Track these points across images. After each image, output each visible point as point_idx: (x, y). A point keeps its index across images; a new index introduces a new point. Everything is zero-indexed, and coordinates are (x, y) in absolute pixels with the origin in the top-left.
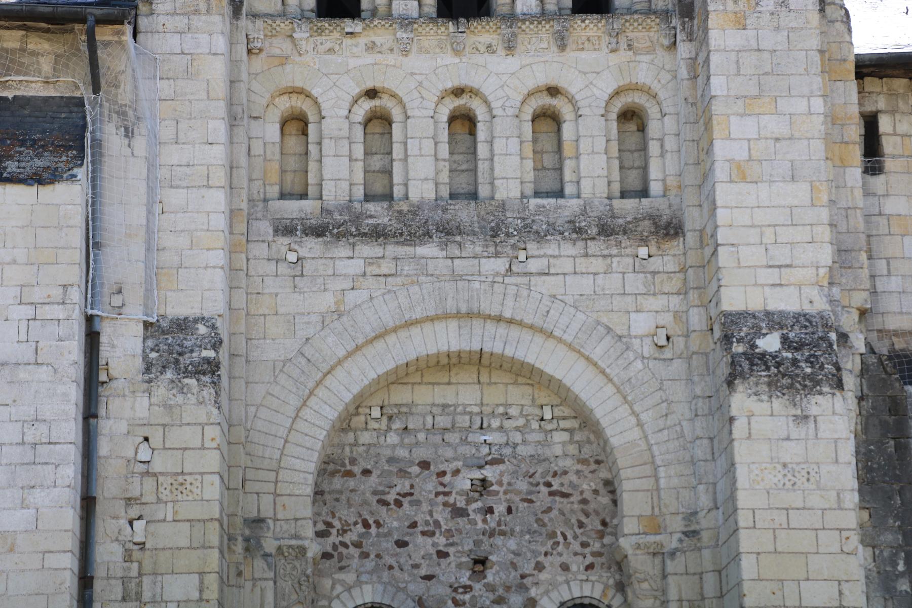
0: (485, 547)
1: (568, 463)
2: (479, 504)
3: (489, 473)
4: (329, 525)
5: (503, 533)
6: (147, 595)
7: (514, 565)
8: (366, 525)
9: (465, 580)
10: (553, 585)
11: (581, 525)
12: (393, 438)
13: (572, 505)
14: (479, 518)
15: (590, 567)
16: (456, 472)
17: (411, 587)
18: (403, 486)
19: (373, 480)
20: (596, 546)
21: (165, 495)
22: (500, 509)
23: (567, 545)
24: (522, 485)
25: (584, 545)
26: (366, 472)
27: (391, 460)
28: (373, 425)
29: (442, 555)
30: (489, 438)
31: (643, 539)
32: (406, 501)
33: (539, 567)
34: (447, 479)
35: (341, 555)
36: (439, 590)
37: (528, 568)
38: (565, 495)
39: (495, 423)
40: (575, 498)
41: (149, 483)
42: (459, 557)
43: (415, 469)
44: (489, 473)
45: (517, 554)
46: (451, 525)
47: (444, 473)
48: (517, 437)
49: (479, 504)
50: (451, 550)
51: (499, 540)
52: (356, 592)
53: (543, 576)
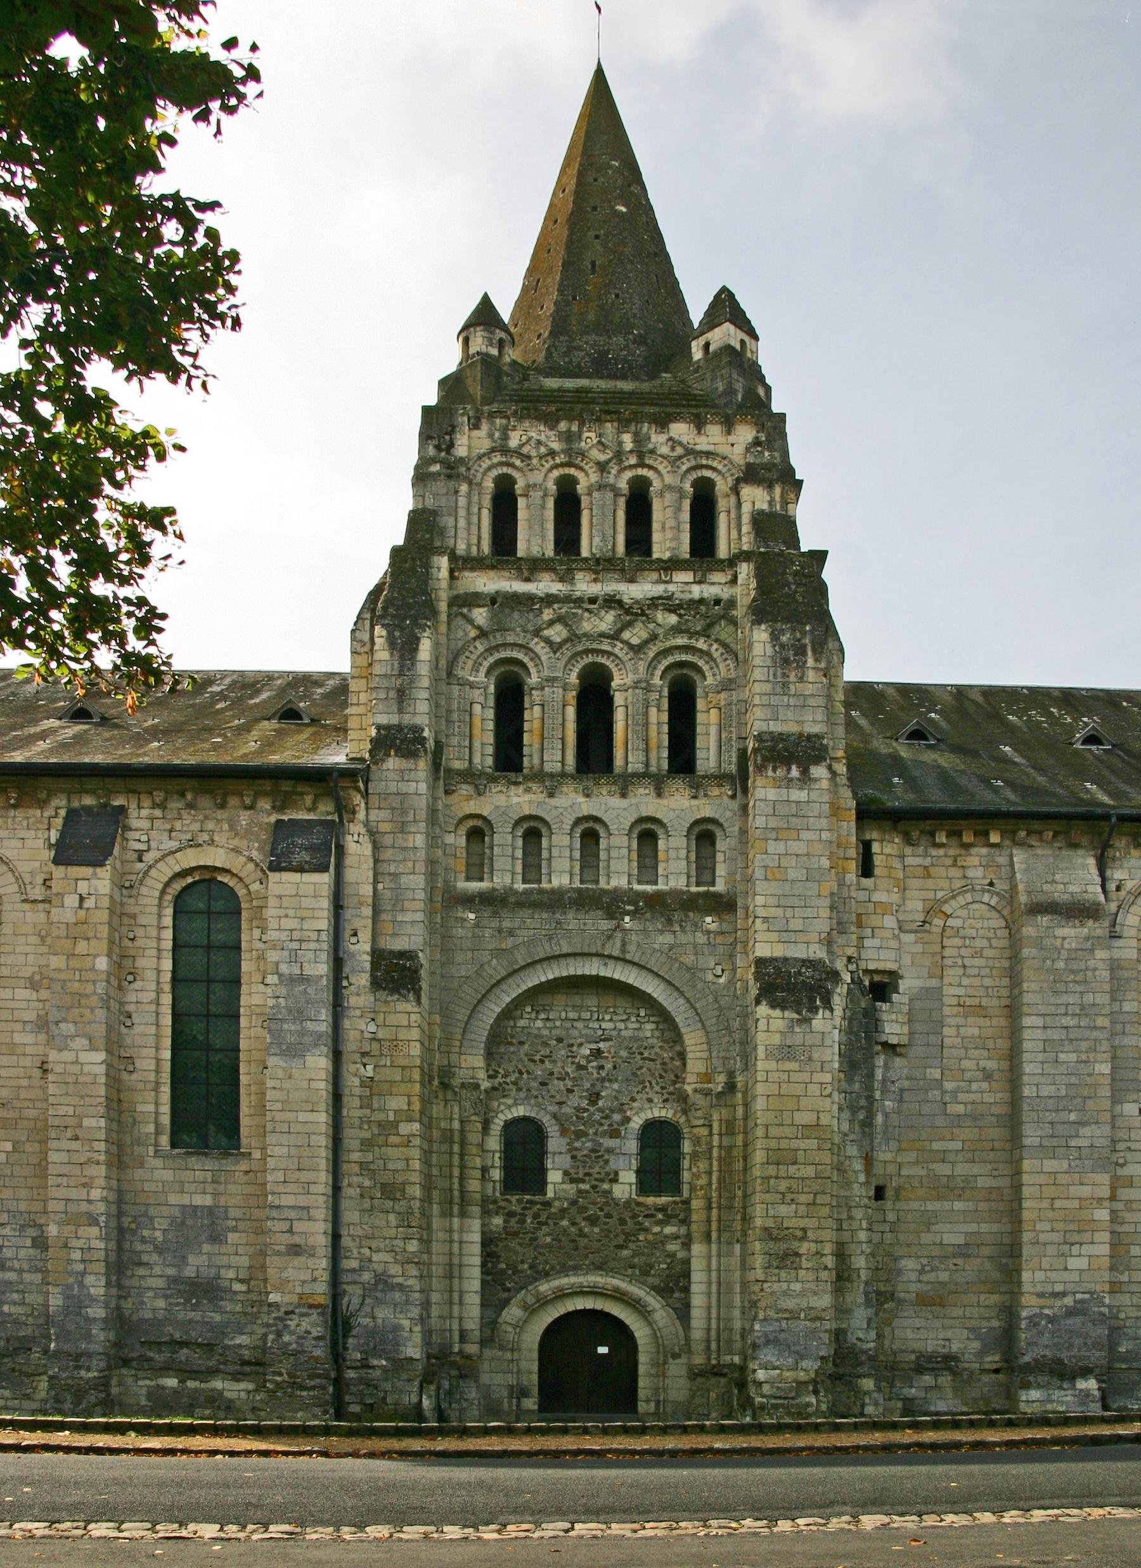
0: (598, 1087)
2: (594, 1064)
3: (601, 1045)
4: (497, 1072)
5: (610, 1081)
7: (616, 1098)
8: (521, 1073)
10: (642, 1109)
11: (661, 1077)
12: (539, 1024)
14: (595, 1072)
16: (581, 1045)
22: (609, 1066)
23: (652, 1087)
24: (624, 1053)
29: (570, 1091)
30: (604, 1025)
33: (633, 1100)
35: (504, 1090)
36: (566, 1110)
39: (607, 1017)
44: (601, 1045)
45: (618, 1092)
49: (594, 1064)
51: (607, 1084)
52: (513, 1109)
53: (635, 1105)
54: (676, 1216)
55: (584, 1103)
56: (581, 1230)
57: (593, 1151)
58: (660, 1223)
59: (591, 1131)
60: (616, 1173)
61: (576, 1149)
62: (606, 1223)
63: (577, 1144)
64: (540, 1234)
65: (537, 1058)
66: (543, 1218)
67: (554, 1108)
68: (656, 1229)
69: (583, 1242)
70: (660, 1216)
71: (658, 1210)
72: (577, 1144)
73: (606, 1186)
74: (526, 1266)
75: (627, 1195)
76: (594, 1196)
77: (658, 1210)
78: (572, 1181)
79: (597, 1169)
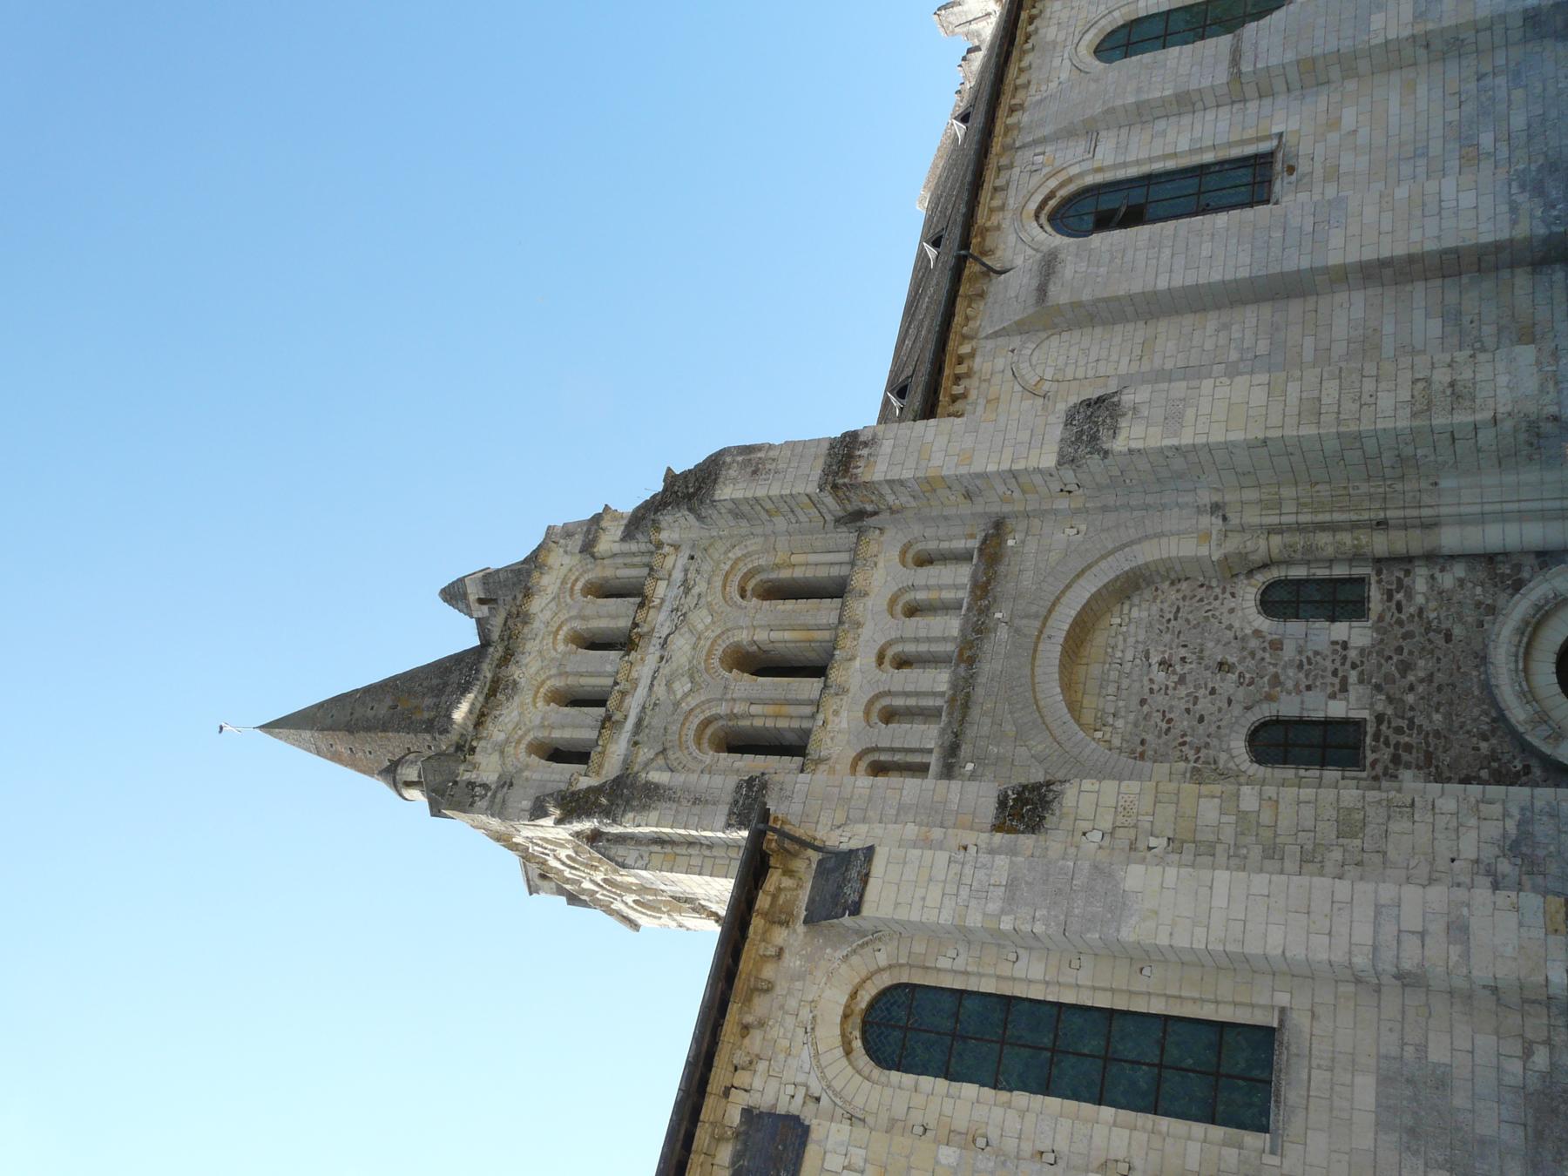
1: (1155, 609)
3: (1155, 660)
5: (1202, 651)
6: (1212, 838)
9: (1234, 677)
11: (1201, 600)
13: (1186, 607)
14: (1188, 667)
15: (1233, 595)
16: (1151, 681)
17: (1236, 713)
18: (1157, 717)
19: (1149, 737)
20: (1218, 591)
21: (1131, 821)
22: (1183, 652)
24: (1167, 637)
25: (1216, 598)
26: (1143, 742)
27: (1136, 725)
28: (1107, 737)
29: (1213, 692)
31: (1213, 543)
32: (1168, 716)
33: (1230, 627)
34: (1155, 687)
37: (1230, 634)
38: (1178, 609)
39: (1119, 654)
40: (1181, 603)
41: (1120, 833)
42: (1215, 681)
43: (1146, 708)
44: (1155, 660)
45: (1218, 641)
46: (1191, 685)
47: (1151, 691)
48: (1131, 640)
50: (1210, 685)
51: (1206, 653)
52: (1235, 753)
53: (1237, 625)
54: (1399, 579)
55: (1233, 677)
56: (1421, 681)
57: (1300, 666)
58: (1410, 596)
59: (1272, 669)
60: (1334, 643)
61: (1297, 685)
62: (1411, 653)
63: (1290, 684)
64: (1427, 726)
65: (1164, 726)
66: (1404, 724)
67: (1237, 710)
68: (1420, 600)
69: (1440, 677)
70: (1399, 596)
71: (1390, 598)
72: (1290, 684)
73: (1353, 654)
74: (1484, 745)
75: (1369, 632)
76: (1366, 667)
77: (1390, 598)
78: (1344, 688)
79: (1328, 663)
